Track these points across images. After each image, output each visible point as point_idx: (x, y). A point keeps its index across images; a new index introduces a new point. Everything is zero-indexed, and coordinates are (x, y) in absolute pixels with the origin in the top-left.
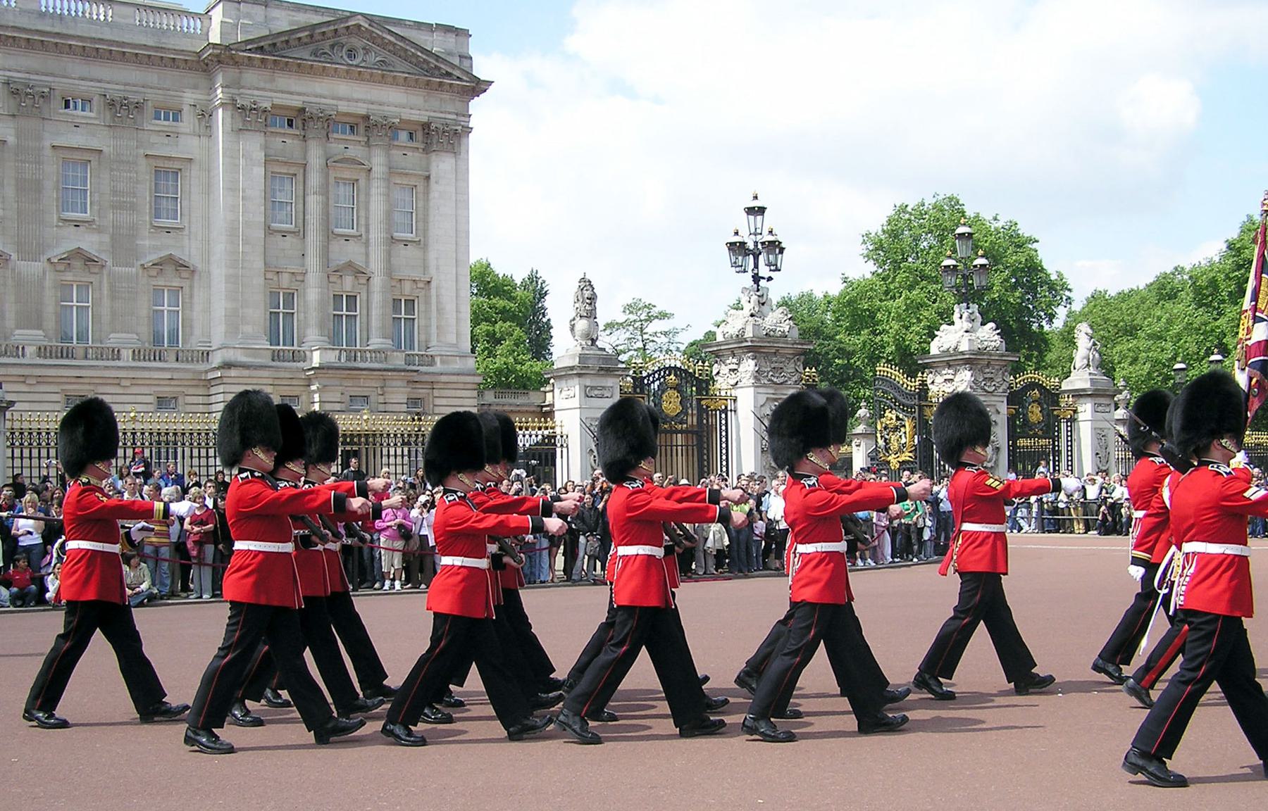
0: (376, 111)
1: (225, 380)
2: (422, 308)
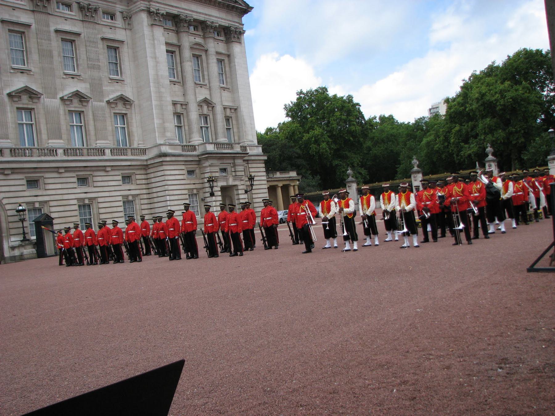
0: (209, 19)
1: (164, 163)
2: (234, 122)
